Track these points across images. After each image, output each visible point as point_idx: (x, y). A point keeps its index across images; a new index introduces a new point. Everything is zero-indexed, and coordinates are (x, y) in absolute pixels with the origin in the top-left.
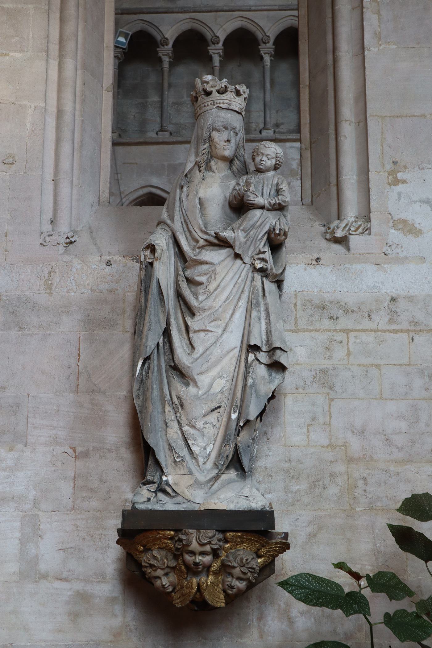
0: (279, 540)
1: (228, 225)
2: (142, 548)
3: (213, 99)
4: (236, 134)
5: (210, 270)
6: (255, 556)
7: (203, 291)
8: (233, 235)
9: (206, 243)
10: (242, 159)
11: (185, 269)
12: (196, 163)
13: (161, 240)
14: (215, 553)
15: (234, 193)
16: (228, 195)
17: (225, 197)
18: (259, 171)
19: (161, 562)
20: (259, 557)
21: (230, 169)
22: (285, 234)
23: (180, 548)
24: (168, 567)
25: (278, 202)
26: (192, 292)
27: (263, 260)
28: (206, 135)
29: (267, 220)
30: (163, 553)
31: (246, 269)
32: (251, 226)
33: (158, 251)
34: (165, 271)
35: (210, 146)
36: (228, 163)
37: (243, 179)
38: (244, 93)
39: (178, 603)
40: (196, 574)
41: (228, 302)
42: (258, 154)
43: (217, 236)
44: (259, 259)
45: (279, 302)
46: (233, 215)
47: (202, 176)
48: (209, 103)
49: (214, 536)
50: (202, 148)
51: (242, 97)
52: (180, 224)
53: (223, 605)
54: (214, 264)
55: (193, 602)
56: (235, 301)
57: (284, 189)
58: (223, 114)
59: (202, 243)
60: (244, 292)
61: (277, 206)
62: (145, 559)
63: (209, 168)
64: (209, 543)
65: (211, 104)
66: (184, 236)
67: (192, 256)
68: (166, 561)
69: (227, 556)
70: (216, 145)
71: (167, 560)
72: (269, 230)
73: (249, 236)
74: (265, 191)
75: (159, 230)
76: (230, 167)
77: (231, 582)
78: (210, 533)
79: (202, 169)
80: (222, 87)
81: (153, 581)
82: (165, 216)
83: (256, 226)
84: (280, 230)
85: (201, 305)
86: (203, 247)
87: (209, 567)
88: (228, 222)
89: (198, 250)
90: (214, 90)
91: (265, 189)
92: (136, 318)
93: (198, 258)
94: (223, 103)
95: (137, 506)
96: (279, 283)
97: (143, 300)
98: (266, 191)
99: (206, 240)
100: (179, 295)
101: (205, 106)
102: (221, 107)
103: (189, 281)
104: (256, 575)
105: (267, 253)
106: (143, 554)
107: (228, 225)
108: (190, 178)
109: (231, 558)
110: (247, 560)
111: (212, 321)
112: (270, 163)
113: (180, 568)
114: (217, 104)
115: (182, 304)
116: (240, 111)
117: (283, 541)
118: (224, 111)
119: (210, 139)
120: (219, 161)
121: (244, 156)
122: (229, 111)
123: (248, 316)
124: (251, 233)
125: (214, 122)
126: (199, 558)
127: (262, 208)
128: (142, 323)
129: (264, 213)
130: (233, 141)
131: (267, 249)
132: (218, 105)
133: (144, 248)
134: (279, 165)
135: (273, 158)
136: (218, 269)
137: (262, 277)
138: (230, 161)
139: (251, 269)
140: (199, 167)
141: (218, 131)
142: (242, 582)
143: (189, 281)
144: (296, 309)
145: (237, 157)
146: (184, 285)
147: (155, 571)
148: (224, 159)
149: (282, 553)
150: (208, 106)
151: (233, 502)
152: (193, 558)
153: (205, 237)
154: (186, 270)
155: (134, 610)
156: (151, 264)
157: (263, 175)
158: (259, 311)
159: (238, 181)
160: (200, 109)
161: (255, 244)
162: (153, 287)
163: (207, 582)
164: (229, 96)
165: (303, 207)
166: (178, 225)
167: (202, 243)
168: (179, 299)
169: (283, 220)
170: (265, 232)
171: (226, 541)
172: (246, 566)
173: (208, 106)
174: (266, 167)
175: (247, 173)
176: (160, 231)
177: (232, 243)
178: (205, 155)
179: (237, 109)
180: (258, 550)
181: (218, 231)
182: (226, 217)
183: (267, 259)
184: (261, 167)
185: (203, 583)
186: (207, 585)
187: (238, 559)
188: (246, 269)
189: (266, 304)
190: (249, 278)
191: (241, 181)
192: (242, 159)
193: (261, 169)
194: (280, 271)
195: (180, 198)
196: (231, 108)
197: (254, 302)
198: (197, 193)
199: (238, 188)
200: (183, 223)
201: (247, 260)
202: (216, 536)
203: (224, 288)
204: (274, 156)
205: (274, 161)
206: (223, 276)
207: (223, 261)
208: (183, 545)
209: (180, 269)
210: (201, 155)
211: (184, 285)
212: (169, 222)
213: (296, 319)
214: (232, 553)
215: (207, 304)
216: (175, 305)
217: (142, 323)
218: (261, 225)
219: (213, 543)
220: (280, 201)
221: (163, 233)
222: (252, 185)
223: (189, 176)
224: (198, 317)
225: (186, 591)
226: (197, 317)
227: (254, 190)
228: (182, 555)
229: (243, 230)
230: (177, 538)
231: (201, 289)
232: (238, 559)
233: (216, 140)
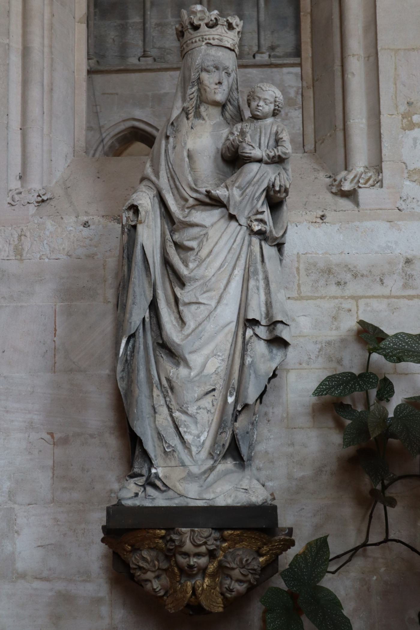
0: (283, 537)
1: (222, 180)
2: (130, 547)
3: (201, 34)
4: (229, 74)
5: (201, 233)
6: (256, 556)
7: (194, 258)
8: (227, 193)
9: (195, 202)
10: (235, 103)
11: (172, 232)
12: (183, 109)
13: (145, 200)
14: (212, 554)
15: (228, 144)
16: (220, 146)
17: (217, 148)
18: (255, 118)
19: (151, 564)
20: (261, 555)
21: (222, 115)
22: (286, 191)
23: (172, 549)
24: (159, 569)
25: (277, 154)
26: (181, 259)
27: (262, 221)
28: (194, 76)
29: (265, 175)
30: (154, 553)
31: (242, 232)
32: (248, 183)
33: (142, 213)
34: (150, 235)
35: (199, 90)
36: (220, 109)
37: (237, 128)
38: (237, 26)
39: (171, 609)
40: (191, 576)
41: (222, 270)
42: (254, 99)
43: (208, 193)
44: (256, 220)
45: (280, 269)
46: (227, 169)
47: (190, 124)
48: (197, 39)
49: (210, 536)
50: (189, 92)
51: (234, 31)
52: (166, 181)
53: (221, 610)
54: (206, 227)
55: (188, 606)
56: (230, 269)
57: (284, 139)
58: (213, 51)
59: (191, 202)
60: (241, 259)
61: (276, 159)
62: (134, 560)
63: (198, 115)
64: (205, 543)
65: (199, 40)
66: (171, 194)
67: (181, 217)
68: (156, 563)
69: (225, 556)
70: (206, 88)
71: (158, 561)
72: (268, 187)
73: (244, 194)
74: (262, 142)
75: (142, 187)
76: (223, 114)
77: (230, 585)
78: (206, 532)
79: (190, 116)
80: (211, 20)
81: (143, 584)
82: (149, 171)
83: (253, 183)
84: (280, 186)
85: (192, 274)
86: (193, 207)
87: (206, 568)
88: (221, 177)
89: (187, 211)
90: (202, 23)
91: (263, 138)
92: (118, 289)
93: (187, 219)
94: (214, 39)
95: (123, 502)
96: (280, 246)
97: (126, 268)
98: (264, 141)
99: (196, 199)
100: (167, 263)
101: (192, 43)
102: (210, 44)
103: (178, 246)
104: (257, 577)
105: (266, 213)
106: (131, 555)
107: (222, 181)
108: (177, 127)
109: (229, 559)
110: (247, 560)
111: (204, 293)
112: (268, 108)
113: (173, 571)
114: (206, 39)
115: (170, 272)
116: (232, 48)
117: (287, 538)
118: (215, 48)
119: (199, 81)
120: (210, 106)
121: (238, 100)
122: (220, 48)
123: (245, 286)
124: (248, 191)
125: (203, 62)
126: (193, 561)
127: (260, 161)
128: (125, 295)
129: (262, 168)
130: (225, 83)
131: (266, 209)
132: (208, 41)
133: (126, 210)
134: (278, 110)
135: (271, 103)
136: (211, 232)
137: (260, 240)
138: (223, 106)
139: (248, 233)
140: (187, 114)
141: (208, 71)
142: (242, 584)
143: (178, 246)
144: (298, 273)
145: (230, 101)
146: (172, 251)
147: (145, 573)
148: (215, 104)
149: (286, 550)
150: (196, 42)
151: (230, 496)
152: (187, 559)
153: (195, 195)
154: (174, 233)
155: (122, 611)
156: (135, 227)
157: (260, 123)
158: (257, 280)
159: (232, 129)
160: (187, 46)
161: (252, 203)
162: (137, 254)
163: (203, 586)
164: (221, 30)
165: (305, 154)
166: (164, 182)
167: (191, 202)
168: (166, 267)
169: (284, 175)
170: (263, 189)
171: (224, 540)
172: (246, 567)
173: (196, 42)
174: (263, 113)
175: (242, 120)
176: (144, 189)
177: (225, 202)
178: (194, 100)
179: (229, 46)
180: (260, 548)
181: (208, 189)
182: (218, 172)
183: (266, 220)
184: (258, 113)
185: (199, 587)
186: (203, 589)
187: (238, 559)
188: (242, 232)
189: (265, 272)
190: (246, 242)
191: (235, 129)
192: (235, 103)
193: (258, 115)
194: (281, 234)
195: (165, 150)
196: (222, 44)
197: (252, 269)
198: (185, 144)
199: (231, 138)
200: (170, 178)
201: (243, 221)
202: (213, 535)
203: (217, 254)
204: (272, 100)
205: (272, 107)
206: (215, 240)
207: (215, 223)
208: (176, 546)
209: (168, 232)
210: (189, 99)
211: (172, 251)
212: (153, 178)
213: (299, 286)
214: (230, 552)
215: (199, 272)
216: (163, 277)
217: (125, 295)
218: (258, 181)
219: (209, 543)
220: (280, 153)
221: (147, 191)
222: (248, 135)
223: (175, 124)
224: (189, 287)
225: (180, 595)
226: (188, 288)
227: (250, 140)
228: (174, 556)
229: (238, 187)
230: (168, 538)
231: (191, 256)
232: (238, 559)
233: (206, 82)
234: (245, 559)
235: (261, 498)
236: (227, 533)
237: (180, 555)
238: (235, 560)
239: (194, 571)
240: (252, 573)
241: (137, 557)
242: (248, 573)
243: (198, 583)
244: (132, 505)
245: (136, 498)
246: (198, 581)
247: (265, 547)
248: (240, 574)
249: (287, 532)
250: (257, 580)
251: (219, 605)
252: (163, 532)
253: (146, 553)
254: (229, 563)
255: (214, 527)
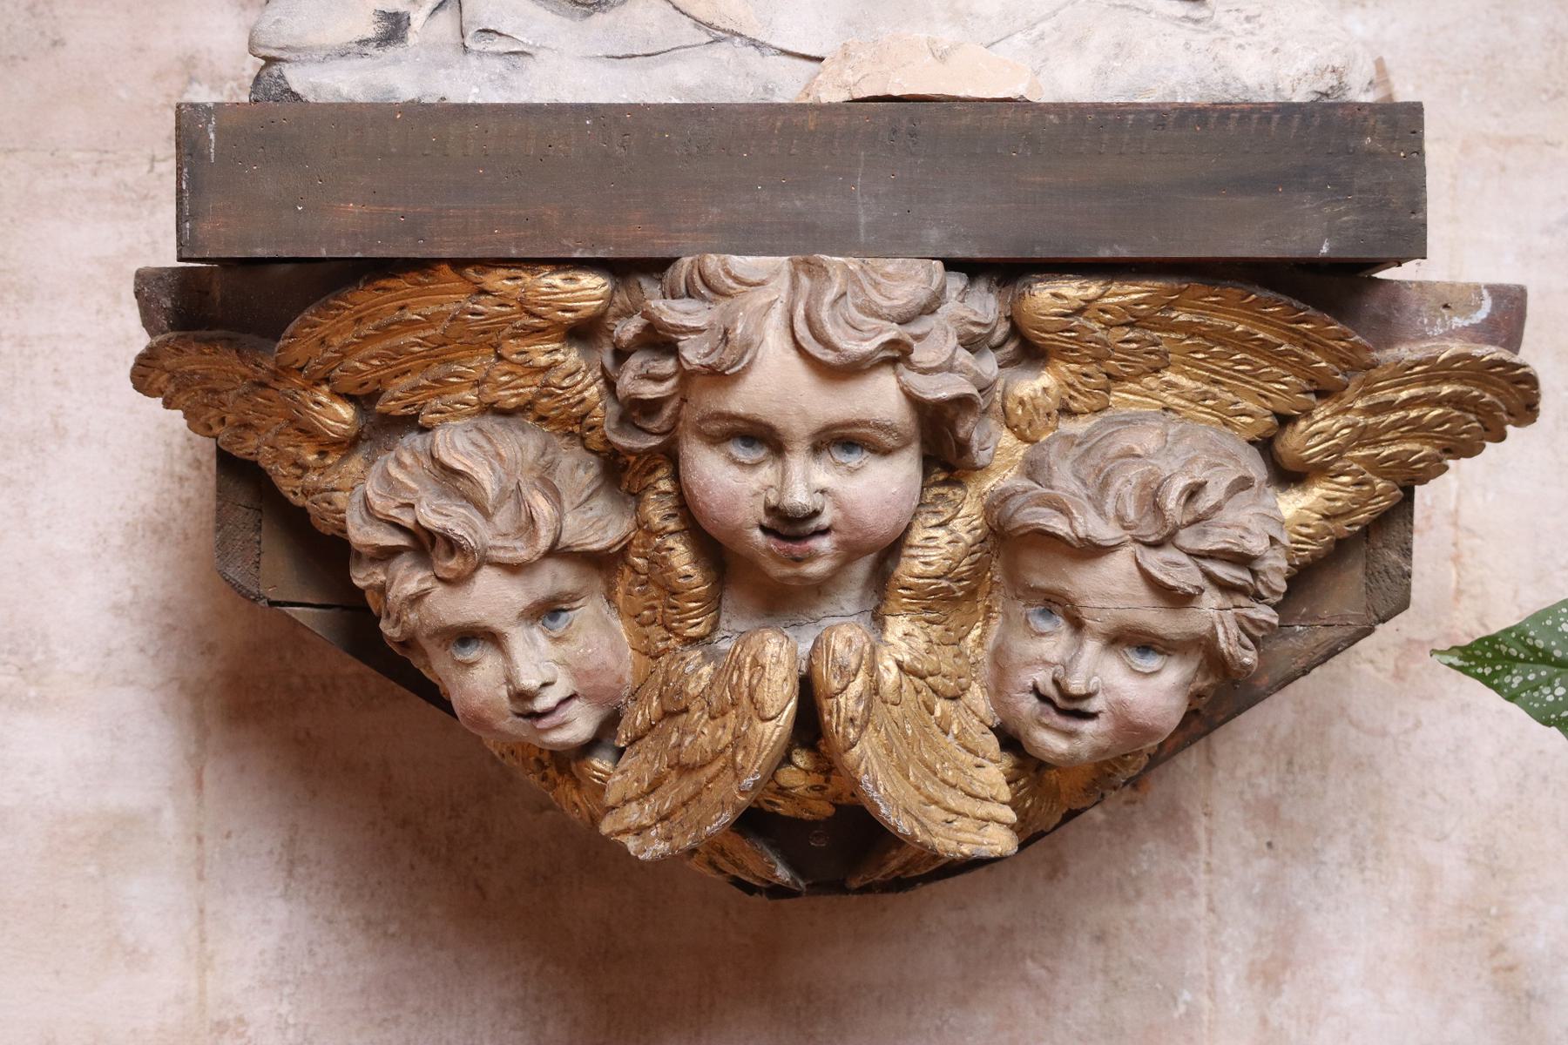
0: (1455, 347)
2: (346, 411)
6: (1257, 469)
14: (942, 443)
19: (503, 518)
20: (1289, 476)
23: (651, 407)
24: (556, 552)
30: (522, 445)
39: (640, 831)
40: (784, 600)
49: (929, 308)
53: (1000, 841)
55: (754, 821)
62: (368, 497)
64: (897, 355)
68: (542, 506)
69: (1032, 469)
71: (554, 495)
77: (1067, 667)
78: (907, 280)
81: (440, 665)
87: (892, 549)
95: (298, 78)
104: (1264, 613)
106: (355, 464)
109: (1065, 481)
110: (1193, 492)
113: (659, 562)
117: (1488, 352)
126: (806, 481)
142: (1152, 663)
147: (456, 582)
149: (1470, 449)
151: (1079, 44)
152: (767, 474)
155: (279, 911)
163: (873, 668)
171: (1028, 349)
172: (1187, 539)
180: (1285, 420)
185: (847, 674)
186: (875, 689)
187: (1126, 483)
202: (952, 307)
208: (686, 377)
214: (1070, 440)
219: (921, 355)
225: (704, 735)
228: (670, 456)
230: (628, 329)
232: (1126, 483)
234: (1180, 483)
235: (1305, 62)
236: (1048, 297)
237: (716, 440)
238: (1105, 485)
239: (812, 557)
240: (1226, 588)
241: (394, 471)
242: (1199, 580)
243: (838, 645)
244: (360, 98)
245: (392, 51)
246: (842, 633)
247: (1322, 411)
248: (1142, 591)
249: (1481, 315)
250: (1257, 635)
251: (983, 810)
252: (592, 286)
253: (461, 442)
254: (1064, 511)
255: (959, 253)
